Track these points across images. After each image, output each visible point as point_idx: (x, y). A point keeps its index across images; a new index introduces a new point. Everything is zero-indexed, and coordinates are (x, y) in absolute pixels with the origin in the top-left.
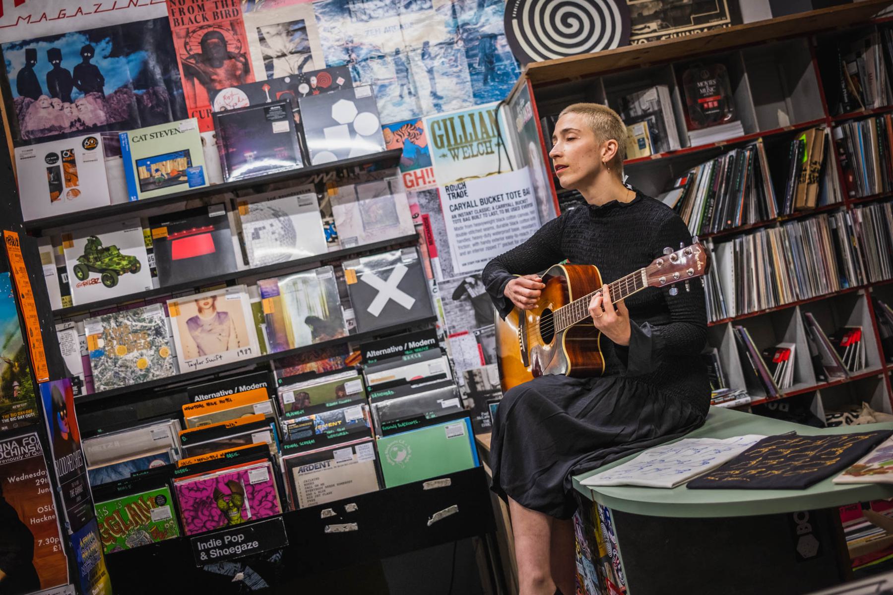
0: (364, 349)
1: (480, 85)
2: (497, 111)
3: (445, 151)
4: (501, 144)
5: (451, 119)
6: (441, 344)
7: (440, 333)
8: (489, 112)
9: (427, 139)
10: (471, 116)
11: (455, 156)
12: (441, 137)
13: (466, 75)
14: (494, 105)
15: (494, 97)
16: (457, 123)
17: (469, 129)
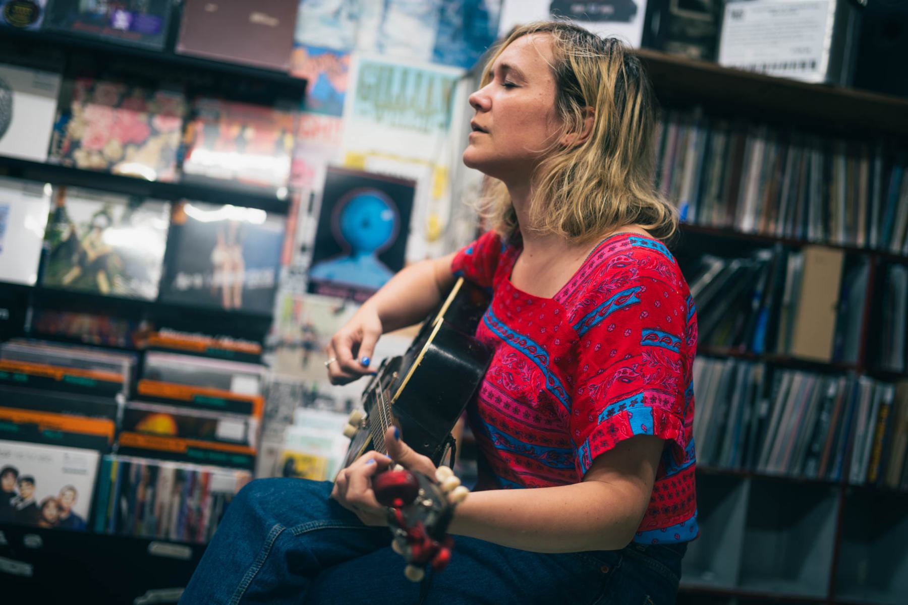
0: (157, 327)
1: (445, 40)
2: (455, 83)
3: (368, 106)
4: (446, 125)
5: (391, 70)
6: (268, 358)
7: (272, 339)
8: (445, 80)
9: (349, 84)
10: (419, 75)
11: (379, 119)
12: (369, 87)
13: (434, 20)
14: (456, 72)
15: (458, 64)
16: (397, 78)
17: (410, 91)
